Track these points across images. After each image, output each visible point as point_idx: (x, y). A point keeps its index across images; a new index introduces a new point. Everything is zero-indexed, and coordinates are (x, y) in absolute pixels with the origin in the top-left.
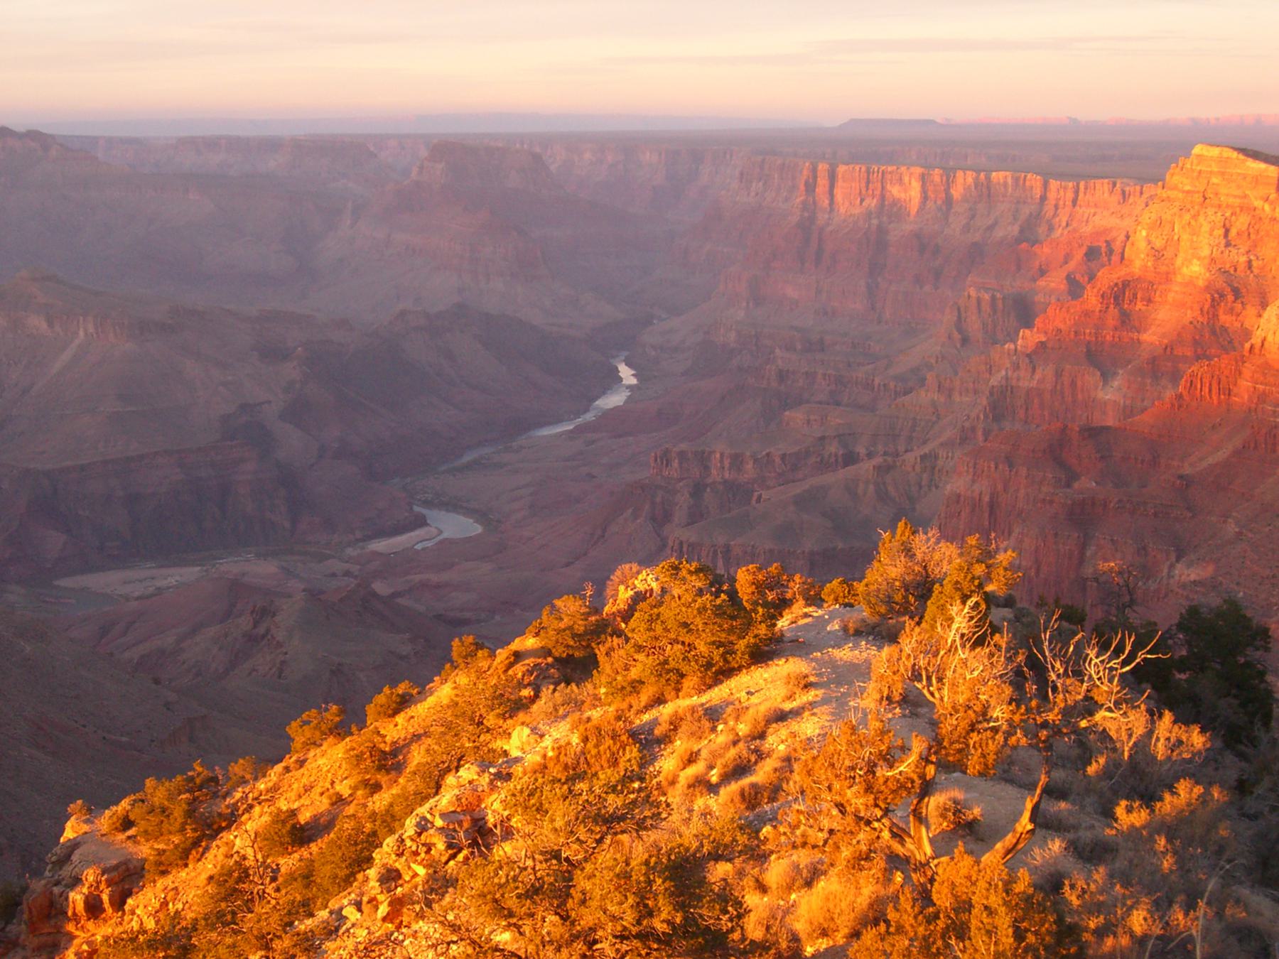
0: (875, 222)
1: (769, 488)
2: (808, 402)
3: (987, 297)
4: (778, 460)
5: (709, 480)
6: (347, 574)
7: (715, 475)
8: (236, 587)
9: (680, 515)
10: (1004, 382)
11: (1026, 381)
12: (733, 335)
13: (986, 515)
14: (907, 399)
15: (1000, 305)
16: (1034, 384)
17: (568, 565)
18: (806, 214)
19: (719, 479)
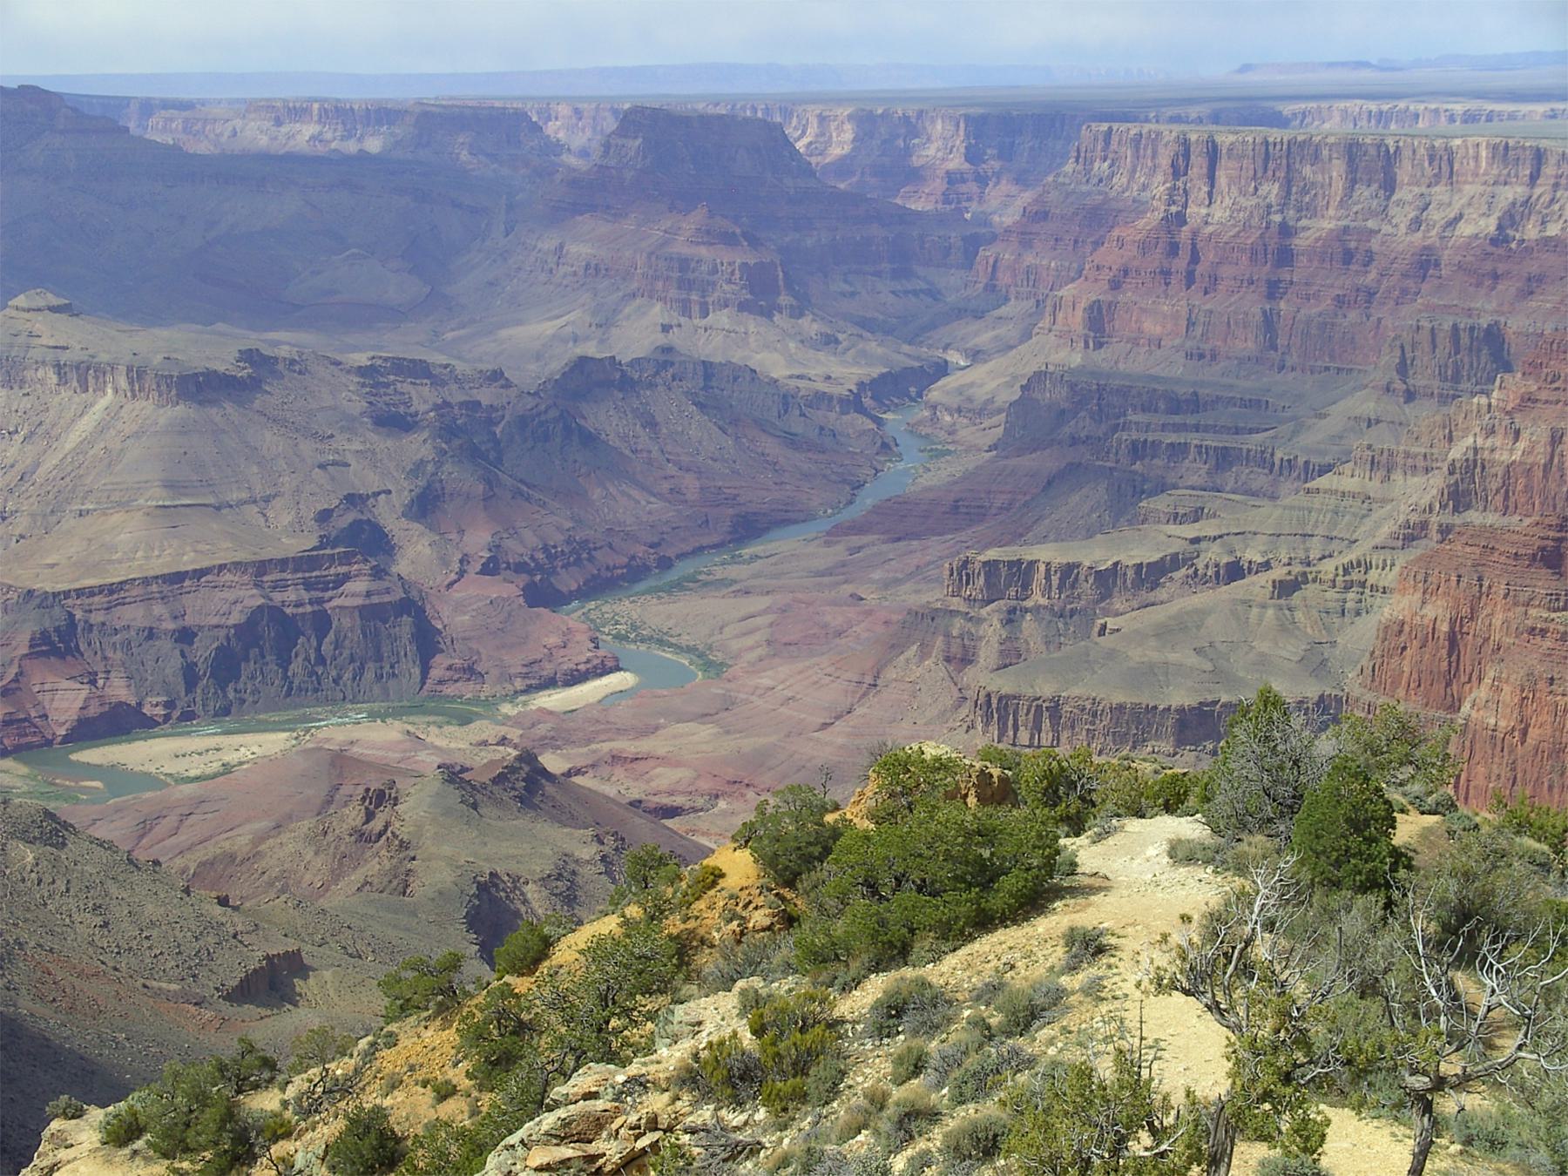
0: (1277, 218)
1: (1117, 614)
2: (1175, 487)
3: (1447, 326)
4: (1130, 574)
5: (1029, 604)
6: (503, 741)
7: (1037, 598)
8: (340, 761)
9: (987, 654)
10: (1471, 455)
11: (1506, 453)
12: (1064, 391)
13: (1444, 652)
14: (1323, 482)
15: (1465, 340)
16: (1517, 456)
17: (825, 726)
18: (1174, 209)
19: (1043, 601)
